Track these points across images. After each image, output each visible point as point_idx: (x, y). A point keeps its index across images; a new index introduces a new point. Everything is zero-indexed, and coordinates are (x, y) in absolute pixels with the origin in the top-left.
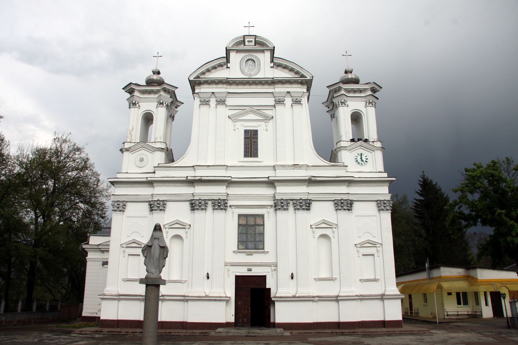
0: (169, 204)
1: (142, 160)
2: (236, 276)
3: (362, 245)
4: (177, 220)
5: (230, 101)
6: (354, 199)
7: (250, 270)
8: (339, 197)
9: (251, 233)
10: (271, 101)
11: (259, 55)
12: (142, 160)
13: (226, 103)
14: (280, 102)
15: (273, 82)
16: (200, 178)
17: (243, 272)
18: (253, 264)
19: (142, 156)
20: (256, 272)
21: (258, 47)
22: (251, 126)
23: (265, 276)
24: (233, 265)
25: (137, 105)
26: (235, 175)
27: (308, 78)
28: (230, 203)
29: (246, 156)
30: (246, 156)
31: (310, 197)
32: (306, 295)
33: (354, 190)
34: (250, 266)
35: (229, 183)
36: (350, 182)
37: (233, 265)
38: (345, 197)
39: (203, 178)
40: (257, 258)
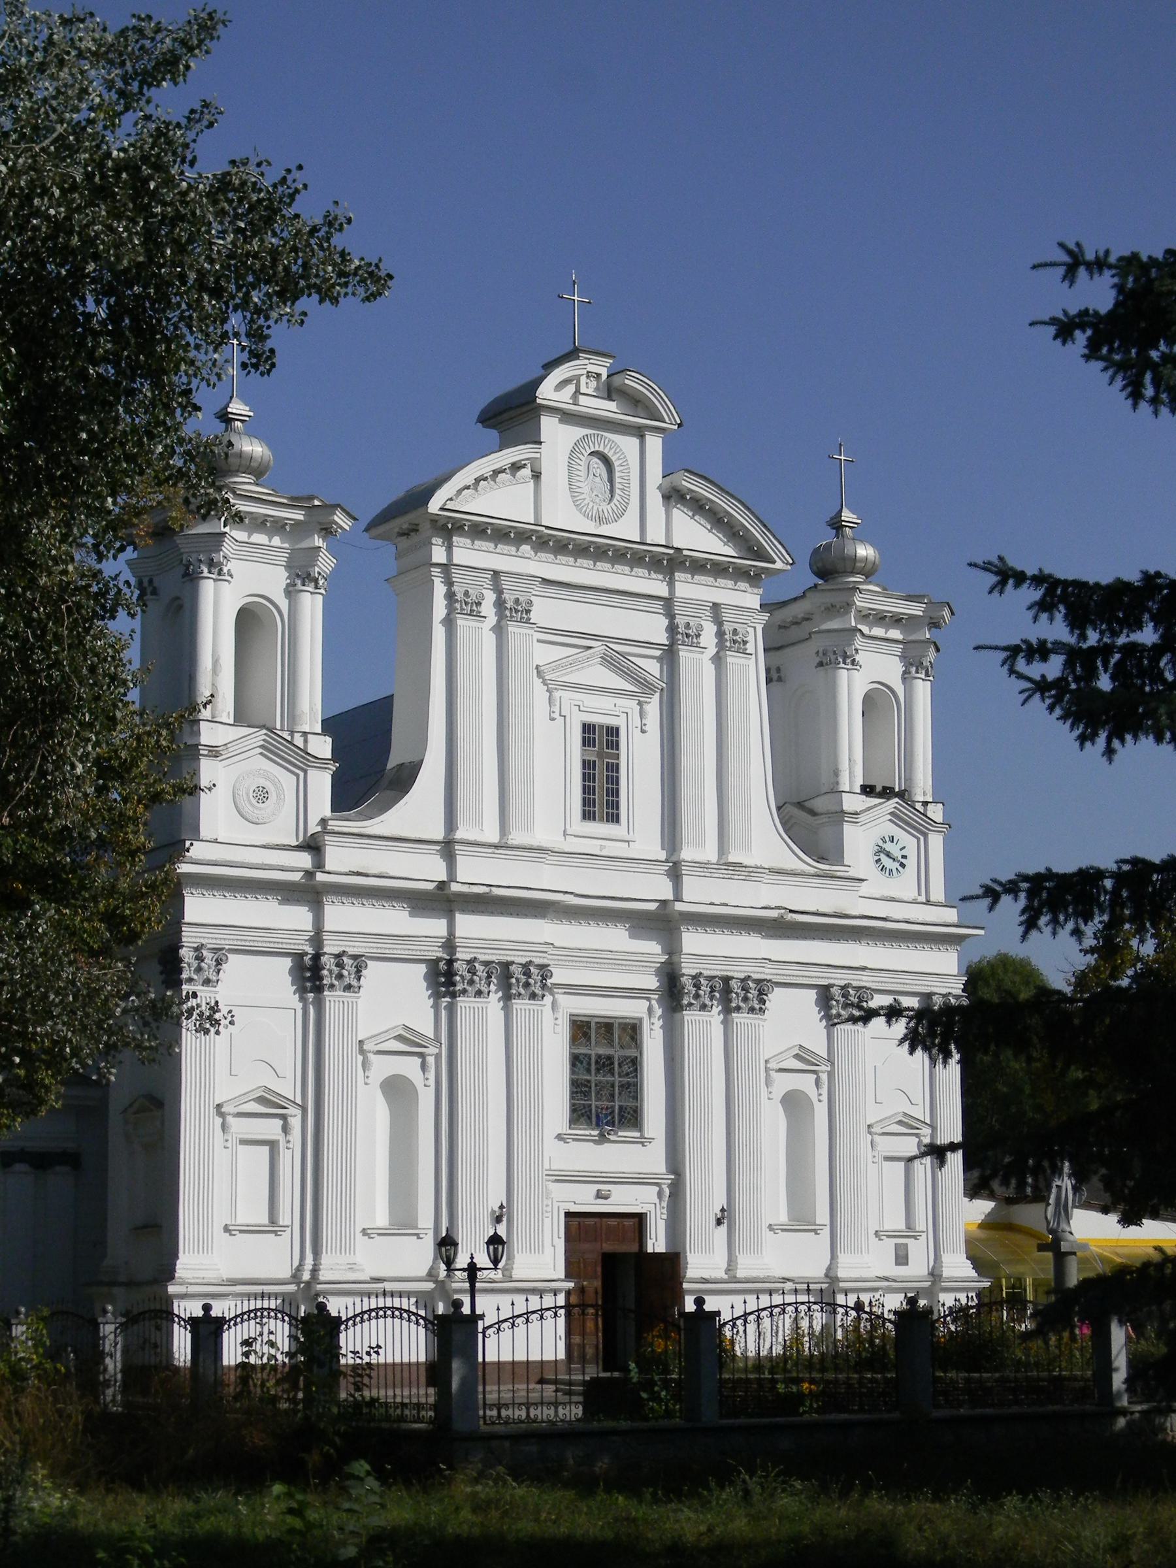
0: (373, 970)
1: (262, 795)
2: (568, 1215)
4: (406, 1027)
8: (838, 979)
9: (605, 1083)
12: (262, 795)
13: (534, 616)
15: (671, 562)
16: (487, 889)
17: (585, 1200)
18: (623, 1173)
19: (262, 782)
20: (623, 1200)
21: (609, 408)
22: (603, 711)
23: (568, 1215)
24: (563, 1178)
27: (779, 565)
29: (588, 815)
30: (588, 815)
31: (766, 973)
32: (761, 1274)
34: (604, 1181)
37: (563, 1178)
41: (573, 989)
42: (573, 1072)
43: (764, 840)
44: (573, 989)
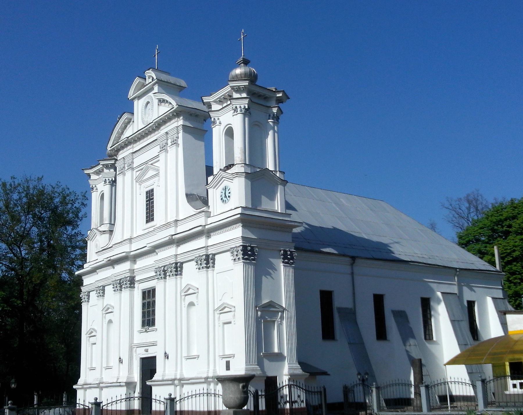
3: (222, 309)
5: (138, 160)
6: (213, 252)
7: (147, 351)
10: (155, 151)
11: (151, 94)
14: (164, 148)
25: (95, 188)
26: (135, 247)
28: (137, 278)
33: (216, 238)
35: (134, 258)
36: (206, 232)
38: (203, 252)
39: (112, 258)
40: (150, 336)
41: (142, 281)
42: (143, 309)
43: (186, 209)
44: (142, 281)
